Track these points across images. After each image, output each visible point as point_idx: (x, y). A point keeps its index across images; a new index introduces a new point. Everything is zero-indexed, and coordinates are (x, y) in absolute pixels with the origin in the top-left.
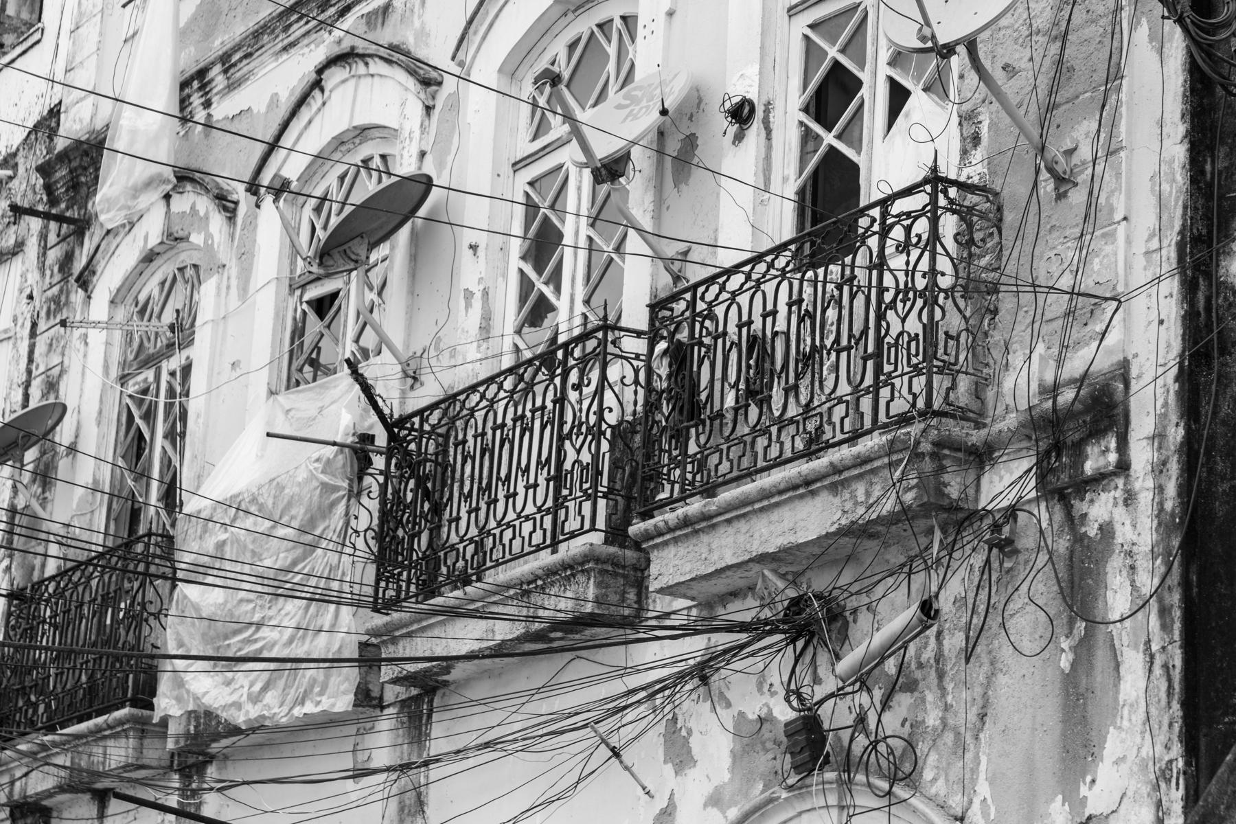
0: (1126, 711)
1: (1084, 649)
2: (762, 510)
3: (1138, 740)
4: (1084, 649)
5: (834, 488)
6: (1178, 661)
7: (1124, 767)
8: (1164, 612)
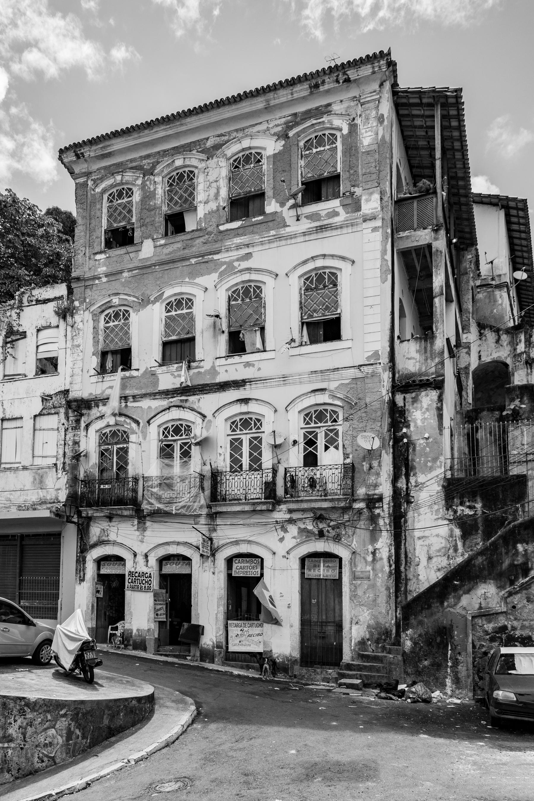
8: (390, 526)
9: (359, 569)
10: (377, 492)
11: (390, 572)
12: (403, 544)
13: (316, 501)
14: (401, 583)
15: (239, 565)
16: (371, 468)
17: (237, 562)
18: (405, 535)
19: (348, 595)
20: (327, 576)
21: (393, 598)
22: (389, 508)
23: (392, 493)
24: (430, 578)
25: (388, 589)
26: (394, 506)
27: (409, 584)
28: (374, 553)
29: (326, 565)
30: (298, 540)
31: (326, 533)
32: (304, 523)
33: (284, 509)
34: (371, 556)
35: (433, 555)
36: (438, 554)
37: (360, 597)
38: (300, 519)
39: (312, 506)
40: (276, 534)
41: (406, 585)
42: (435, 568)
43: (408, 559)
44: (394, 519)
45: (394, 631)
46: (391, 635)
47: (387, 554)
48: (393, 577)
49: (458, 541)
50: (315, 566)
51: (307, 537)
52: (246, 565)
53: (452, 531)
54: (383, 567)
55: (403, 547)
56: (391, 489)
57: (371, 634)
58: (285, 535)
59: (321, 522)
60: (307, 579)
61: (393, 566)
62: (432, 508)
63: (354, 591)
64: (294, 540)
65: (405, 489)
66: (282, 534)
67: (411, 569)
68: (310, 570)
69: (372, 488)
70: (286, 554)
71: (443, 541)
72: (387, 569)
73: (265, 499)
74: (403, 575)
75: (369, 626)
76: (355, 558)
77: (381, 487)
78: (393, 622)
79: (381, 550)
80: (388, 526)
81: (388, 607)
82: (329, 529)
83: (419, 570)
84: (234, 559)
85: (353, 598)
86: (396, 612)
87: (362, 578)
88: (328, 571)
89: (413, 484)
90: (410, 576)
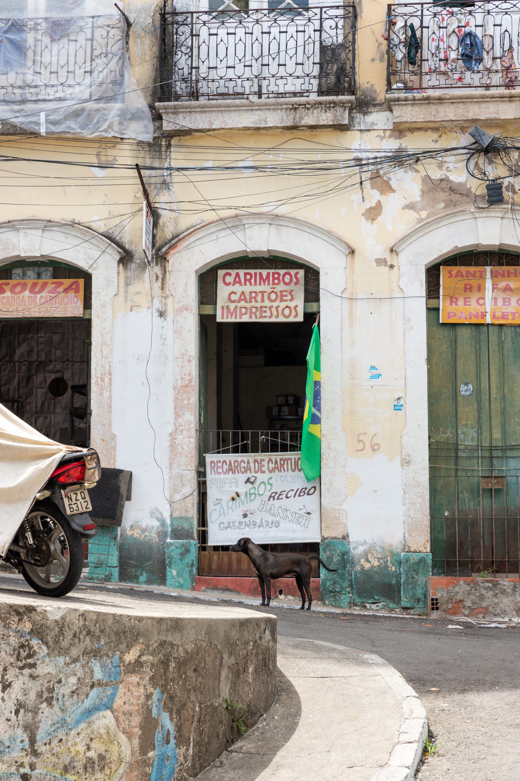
2: (475, 102)
15: (238, 288)
17: (228, 279)
20: (503, 317)
29: (502, 284)
30: (424, 214)
31: (507, 195)
32: (440, 166)
38: (430, 154)
39: (471, 116)
40: (356, 195)
50: (468, 288)
51: (450, 204)
52: (258, 288)
58: (383, 199)
59: (491, 162)
60: (444, 325)
64: (412, 215)
68: (453, 299)
70: (387, 256)
73: (321, 93)
84: (221, 273)
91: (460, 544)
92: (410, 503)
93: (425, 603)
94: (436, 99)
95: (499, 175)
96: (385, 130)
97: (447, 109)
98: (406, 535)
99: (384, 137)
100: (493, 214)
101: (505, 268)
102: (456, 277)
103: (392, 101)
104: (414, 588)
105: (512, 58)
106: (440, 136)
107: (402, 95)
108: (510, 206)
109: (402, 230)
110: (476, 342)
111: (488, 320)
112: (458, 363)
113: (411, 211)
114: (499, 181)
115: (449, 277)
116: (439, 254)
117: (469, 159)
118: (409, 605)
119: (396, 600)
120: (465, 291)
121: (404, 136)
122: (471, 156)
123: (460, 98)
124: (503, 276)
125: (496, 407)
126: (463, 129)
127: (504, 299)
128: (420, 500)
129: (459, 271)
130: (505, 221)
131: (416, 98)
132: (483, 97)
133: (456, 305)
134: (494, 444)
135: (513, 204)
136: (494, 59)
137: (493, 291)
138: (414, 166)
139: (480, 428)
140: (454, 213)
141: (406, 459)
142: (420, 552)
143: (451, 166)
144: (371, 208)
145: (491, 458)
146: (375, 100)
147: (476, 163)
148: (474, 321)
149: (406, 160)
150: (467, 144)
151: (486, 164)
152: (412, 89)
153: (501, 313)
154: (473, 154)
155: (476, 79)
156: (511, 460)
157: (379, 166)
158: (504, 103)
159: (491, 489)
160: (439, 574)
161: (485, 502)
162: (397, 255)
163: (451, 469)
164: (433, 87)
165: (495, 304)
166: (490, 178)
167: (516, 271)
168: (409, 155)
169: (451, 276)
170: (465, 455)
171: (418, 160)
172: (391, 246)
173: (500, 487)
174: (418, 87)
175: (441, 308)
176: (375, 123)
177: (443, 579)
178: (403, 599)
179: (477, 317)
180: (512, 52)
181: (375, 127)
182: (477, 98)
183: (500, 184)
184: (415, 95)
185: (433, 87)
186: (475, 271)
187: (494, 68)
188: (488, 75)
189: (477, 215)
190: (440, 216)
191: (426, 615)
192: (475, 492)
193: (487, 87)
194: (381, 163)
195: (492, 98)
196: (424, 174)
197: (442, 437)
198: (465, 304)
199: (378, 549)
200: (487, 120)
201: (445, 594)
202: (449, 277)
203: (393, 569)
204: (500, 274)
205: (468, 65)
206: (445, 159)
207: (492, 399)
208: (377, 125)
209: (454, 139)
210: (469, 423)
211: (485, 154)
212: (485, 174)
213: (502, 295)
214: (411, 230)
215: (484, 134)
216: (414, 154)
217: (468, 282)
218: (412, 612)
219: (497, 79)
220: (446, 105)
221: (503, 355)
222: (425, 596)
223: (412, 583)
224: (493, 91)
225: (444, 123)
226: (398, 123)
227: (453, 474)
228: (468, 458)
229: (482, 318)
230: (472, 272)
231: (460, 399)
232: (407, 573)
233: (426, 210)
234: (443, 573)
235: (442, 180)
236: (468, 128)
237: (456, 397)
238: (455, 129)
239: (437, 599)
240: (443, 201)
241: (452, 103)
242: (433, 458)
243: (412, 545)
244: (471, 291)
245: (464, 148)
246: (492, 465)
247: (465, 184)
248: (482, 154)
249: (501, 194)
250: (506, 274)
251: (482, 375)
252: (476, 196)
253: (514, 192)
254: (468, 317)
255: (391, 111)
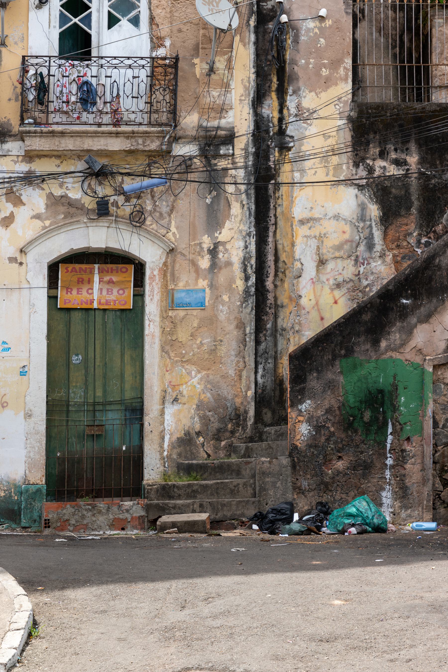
0: (233, 217)
1: (216, 199)
2: (89, 136)
3: (238, 225)
4: (216, 199)
5: (127, 138)
6: (253, 207)
7: (233, 231)
8: (248, 195)
9: (181, 285)
10: (223, 122)
11: (247, 291)
12: (271, 234)
13: (95, 134)
14: (267, 314)
16: (212, 70)
18: (275, 215)
19: (157, 341)
20: (107, 303)
21: (251, 344)
22: (246, 157)
23: (252, 127)
24: (321, 301)
25: (241, 326)
26: (257, 155)
27: (282, 314)
28: (213, 252)
30: (47, 223)
31: (112, 209)
32: (61, 185)
33: (15, 152)
34: (207, 257)
35: (329, 256)
36: (337, 254)
37: (182, 345)
38: (53, 176)
39: (86, 147)
41: (276, 317)
42: (332, 282)
43: (281, 265)
44: (256, 180)
45: (252, 413)
46: (245, 420)
47: (241, 254)
48: (252, 301)
49: (374, 229)
51: (68, 215)
53: (363, 207)
54: (232, 281)
55: (270, 239)
56: (251, 118)
57: (205, 420)
58: (15, 210)
59: (100, 184)
61: (253, 279)
62: (327, 162)
63: (171, 333)
64: (38, 223)
65: (276, 121)
66: (9, 208)
67: (286, 285)
69: (212, 115)
71: (347, 228)
72: (240, 284)
74: (270, 296)
75: (198, 407)
76: (174, 261)
77: (231, 113)
78: (251, 393)
79: (228, 246)
80: (244, 196)
81: (241, 365)
82: (121, 199)
83: (301, 286)
85: (167, 348)
86: (256, 372)
87: (189, 305)
88: (109, 291)
89: (293, 111)
90: (283, 299)
91: (69, 476)
92: (30, 447)
93: (40, 523)
94: (59, 133)
95: (107, 193)
96: (18, 156)
97: (68, 141)
98: (27, 472)
99: (18, 161)
100: (101, 224)
101: (110, 266)
102: (71, 272)
103: (24, 133)
104: (31, 512)
105: (119, 103)
106: (62, 162)
107: (32, 129)
108: (114, 218)
109: (30, 235)
110: (85, 323)
111: (95, 305)
112: (71, 339)
113: (37, 220)
114: (106, 199)
115: (66, 272)
116: (58, 254)
117: (83, 181)
118: (27, 525)
119: (18, 522)
120: (78, 283)
121: (33, 161)
122: (85, 179)
123: (78, 132)
124: (108, 272)
125: (99, 372)
126: (79, 157)
127: (108, 289)
128: (39, 445)
129: (74, 268)
130: (110, 229)
131: (44, 131)
132: (96, 132)
133: (71, 294)
134: (97, 400)
135: (116, 217)
136: (105, 103)
137: (99, 283)
138: (41, 185)
139: (87, 388)
140: (71, 223)
141: (28, 413)
142: (37, 484)
143: (70, 186)
144: (6, 217)
145: (94, 411)
146: (11, 131)
147: (89, 184)
148: (84, 306)
149: (35, 181)
150: (83, 169)
151: (97, 185)
152: (40, 124)
153: (105, 301)
154: (87, 176)
155: (90, 118)
156: (110, 412)
157: (13, 184)
158: (112, 138)
159: (93, 435)
160: (51, 501)
161: (88, 445)
162: (26, 254)
163: (63, 420)
164: (57, 123)
165: (101, 293)
166: (100, 196)
167: (117, 268)
168: (37, 177)
169: (68, 271)
170: (74, 409)
171: (43, 180)
172: (21, 247)
173: (100, 433)
174: (45, 123)
175: (59, 296)
176: (10, 150)
177: (55, 504)
178: (23, 521)
179: (87, 303)
180: (119, 98)
181: (10, 153)
182: (91, 133)
183: (107, 201)
184: (42, 129)
185: (57, 123)
186: (86, 268)
187: (105, 110)
188: (100, 115)
189: (89, 225)
190: (60, 224)
191: (41, 532)
192: (81, 437)
193: (100, 125)
194: (14, 182)
195: (103, 133)
196: (48, 191)
197: (56, 395)
198: (78, 293)
199: (4, 483)
200: (98, 151)
201: (55, 516)
202: (66, 272)
203: (16, 498)
204: (105, 270)
205: (84, 107)
206: (65, 180)
207: (96, 366)
208: (12, 151)
209: (73, 165)
210: (78, 384)
211: (96, 177)
212: (95, 193)
213: (107, 286)
214: (37, 235)
215: (96, 162)
216: (41, 176)
217: (80, 276)
218: (30, 530)
219: (107, 119)
220: (67, 138)
221: (106, 333)
222: (40, 517)
223: (30, 508)
224: (104, 128)
225: (65, 152)
226: (28, 150)
227: (65, 424)
228: (77, 411)
229: (91, 304)
230: (84, 268)
231: (71, 366)
232: (26, 500)
233: (49, 220)
234: (55, 499)
235: (62, 197)
236: (83, 156)
237: (69, 365)
238: (73, 157)
239: (49, 520)
240: (63, 213)
241: (72, 136)
242: (49, 412)
243: (31, 479)
244: (83, 283)
245: (80, 172)
246: (94, 416)
247: (80, 200)
248: (94, 177)
249: (107, 209)
250: (110, 270)
251: (89, 348)
252: (88, 210)
253: (118, 207)
254: (80, 304)
255: (23, 141)
